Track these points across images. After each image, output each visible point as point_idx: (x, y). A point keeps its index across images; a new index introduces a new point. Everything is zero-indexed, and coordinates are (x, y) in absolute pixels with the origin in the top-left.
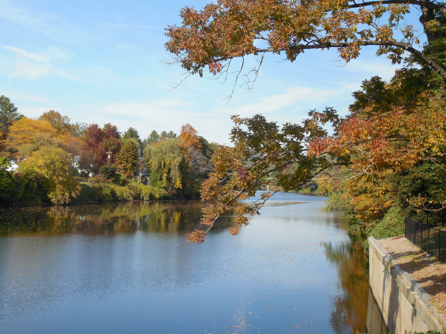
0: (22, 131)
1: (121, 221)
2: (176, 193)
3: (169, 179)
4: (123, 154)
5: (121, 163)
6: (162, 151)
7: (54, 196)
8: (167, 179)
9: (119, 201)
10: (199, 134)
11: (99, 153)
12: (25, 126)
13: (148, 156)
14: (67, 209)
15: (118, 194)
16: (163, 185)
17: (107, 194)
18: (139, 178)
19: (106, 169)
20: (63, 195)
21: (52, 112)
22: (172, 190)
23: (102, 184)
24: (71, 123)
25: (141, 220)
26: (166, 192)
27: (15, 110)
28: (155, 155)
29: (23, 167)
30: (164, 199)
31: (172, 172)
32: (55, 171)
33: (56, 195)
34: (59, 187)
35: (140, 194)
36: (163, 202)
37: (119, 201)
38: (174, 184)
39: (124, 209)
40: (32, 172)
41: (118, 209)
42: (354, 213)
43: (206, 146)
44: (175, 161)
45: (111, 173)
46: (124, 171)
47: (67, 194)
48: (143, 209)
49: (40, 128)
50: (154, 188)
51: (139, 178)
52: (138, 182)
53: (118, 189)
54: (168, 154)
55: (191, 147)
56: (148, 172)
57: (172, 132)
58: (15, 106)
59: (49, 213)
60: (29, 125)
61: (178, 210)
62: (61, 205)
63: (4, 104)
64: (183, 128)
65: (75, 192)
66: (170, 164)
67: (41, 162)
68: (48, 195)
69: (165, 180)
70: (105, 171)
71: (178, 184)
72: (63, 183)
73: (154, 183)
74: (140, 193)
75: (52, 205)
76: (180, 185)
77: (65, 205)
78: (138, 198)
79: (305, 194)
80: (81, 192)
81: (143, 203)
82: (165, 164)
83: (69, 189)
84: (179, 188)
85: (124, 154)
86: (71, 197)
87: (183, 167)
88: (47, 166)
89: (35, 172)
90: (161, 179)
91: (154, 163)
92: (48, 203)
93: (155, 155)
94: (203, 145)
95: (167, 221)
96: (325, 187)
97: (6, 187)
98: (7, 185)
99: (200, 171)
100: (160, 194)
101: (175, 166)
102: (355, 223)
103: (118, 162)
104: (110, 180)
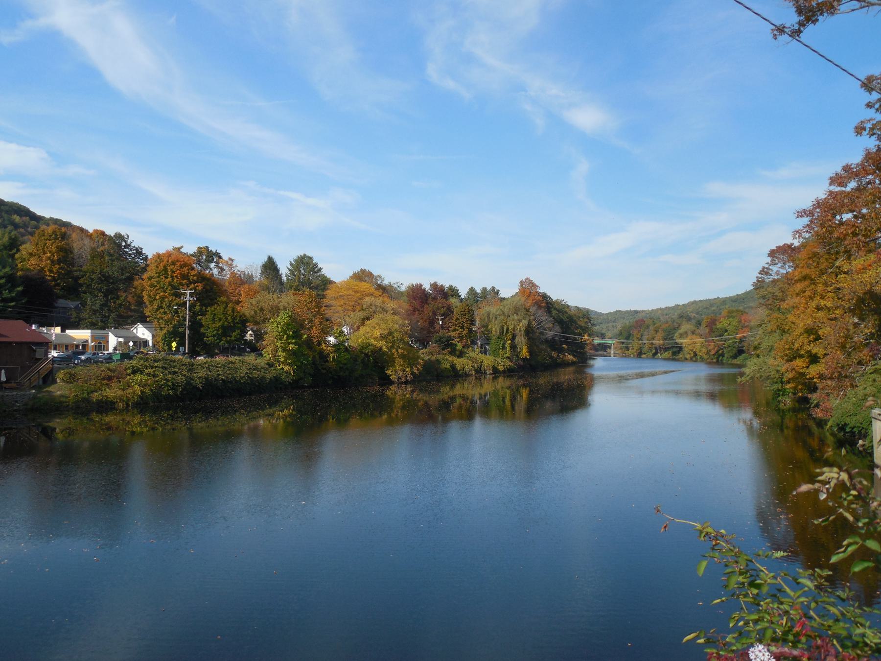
0: (341, 296)
1: (459, 401)
2: (522, 363)
3: (513, 347)
4: (458, 319)
5: (455, 330)
6: (504, 313)
7: (394, 373)
8: (511, 347)
9: (460, 376)
10: (542, 290)
11: (425, 318)
12: (343, 290)
13: (486, 320)
14: (409, 388)
15: (459, 367)
16: (507, 355)
17: (446, 368)
18: (477, 348)
19: (441, 338)
20: (404, 371)
21: (363, 271)
22: (517, 360)
23: (440, 357)
24: (386, 282)
25: (480, 398)
26: (510, 363)
27: (320, 270)
28: (496, 318)
29: (357, 340)
30: (509, 373)
32: (394, 343)
33: (396, 371)
34: (399, 362)
35: (481, 367)
36: (508, 376)
37: (460, 376)
38: (519, 352)
39: (466, 386)
40: (369, 344)
41: (458, 386)
42: (782, 383)
43: (551, 304)
44: (521, 325)
45: (446, 343)
46: (458, 340)
47: (408, 369)
48: (485, 385)
49: (361, 292)
50: (496, 359)
51: (477, 348)
52: (477, 352)
53: (459, 362)
54: (512, 317)
55: (533, 306)
56: (488, 340)
57: (493, 288)
58: (319, 266)
59: (388, 393)
60: (348, 289)
61: (525, 386)
62: (402, 383)
63: (307, 263)
64: (522, 283)
65: (416, 367)
66: (514, 329)
67: (377, 333)
68: (386, 372)
69: (508, 348)
70: (439, 341)
71: (525, 353)
72: (403, 357)
73: (495, 353)
74: (482, 365)
75: (392, 383)
76: (527, 354)
77: (406, 382)
78: (480, 372)
79: (665, 359)
80: (424, 366)
81: (485, 378)
82: (508, 329)
83: (409, 364)
84: (526, 357)
85: (459, 319)
86: (412, 373)
87: (529, 331)
88: (383, 337)
89: (372, 345)
90: (504, 348)
91: (495, 328)
92: (386, 381)
93: (496, 318)
94: (547, 303)
95: (513, 399)
96: (693, 350)
97: (345, 364)
98: (345, 362)
99: (547, 336)
100: (504, 366)
101: (520, 331)
102: (783, 395)
103: (452, 329)
104: (446, 351)
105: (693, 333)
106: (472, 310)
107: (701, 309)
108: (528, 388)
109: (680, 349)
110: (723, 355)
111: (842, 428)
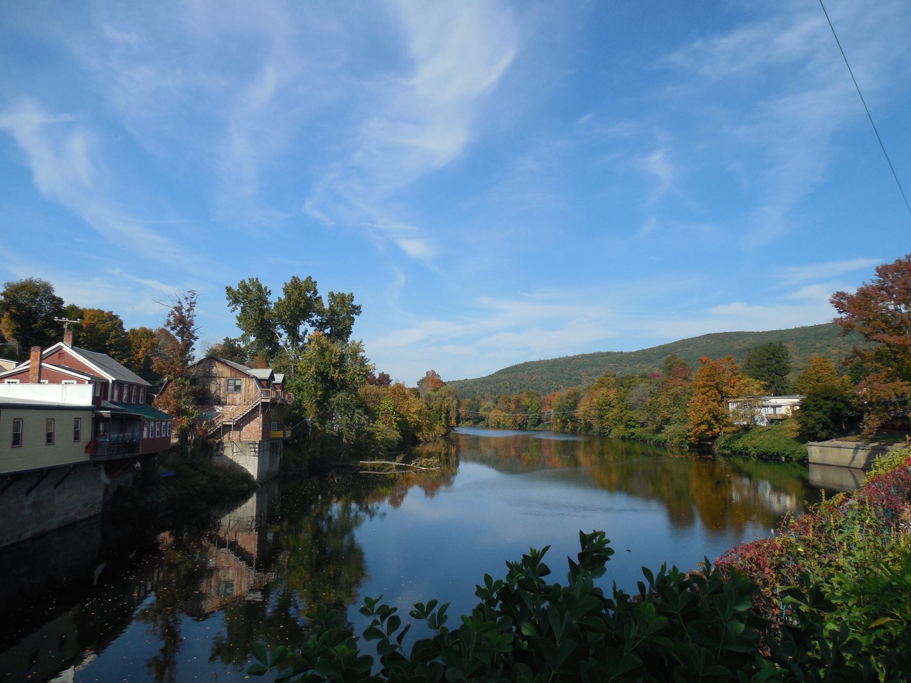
31: (451, 413)
33: (423, 435)
64: (427, 373)
69: (443, 420)
90: (440, 419)
105: (494, 407)
106: (419, 393)
107: (458, 388)
108: (455, 447)
109: (482, 419)
110: (526, 424)
111: (765, 454)
